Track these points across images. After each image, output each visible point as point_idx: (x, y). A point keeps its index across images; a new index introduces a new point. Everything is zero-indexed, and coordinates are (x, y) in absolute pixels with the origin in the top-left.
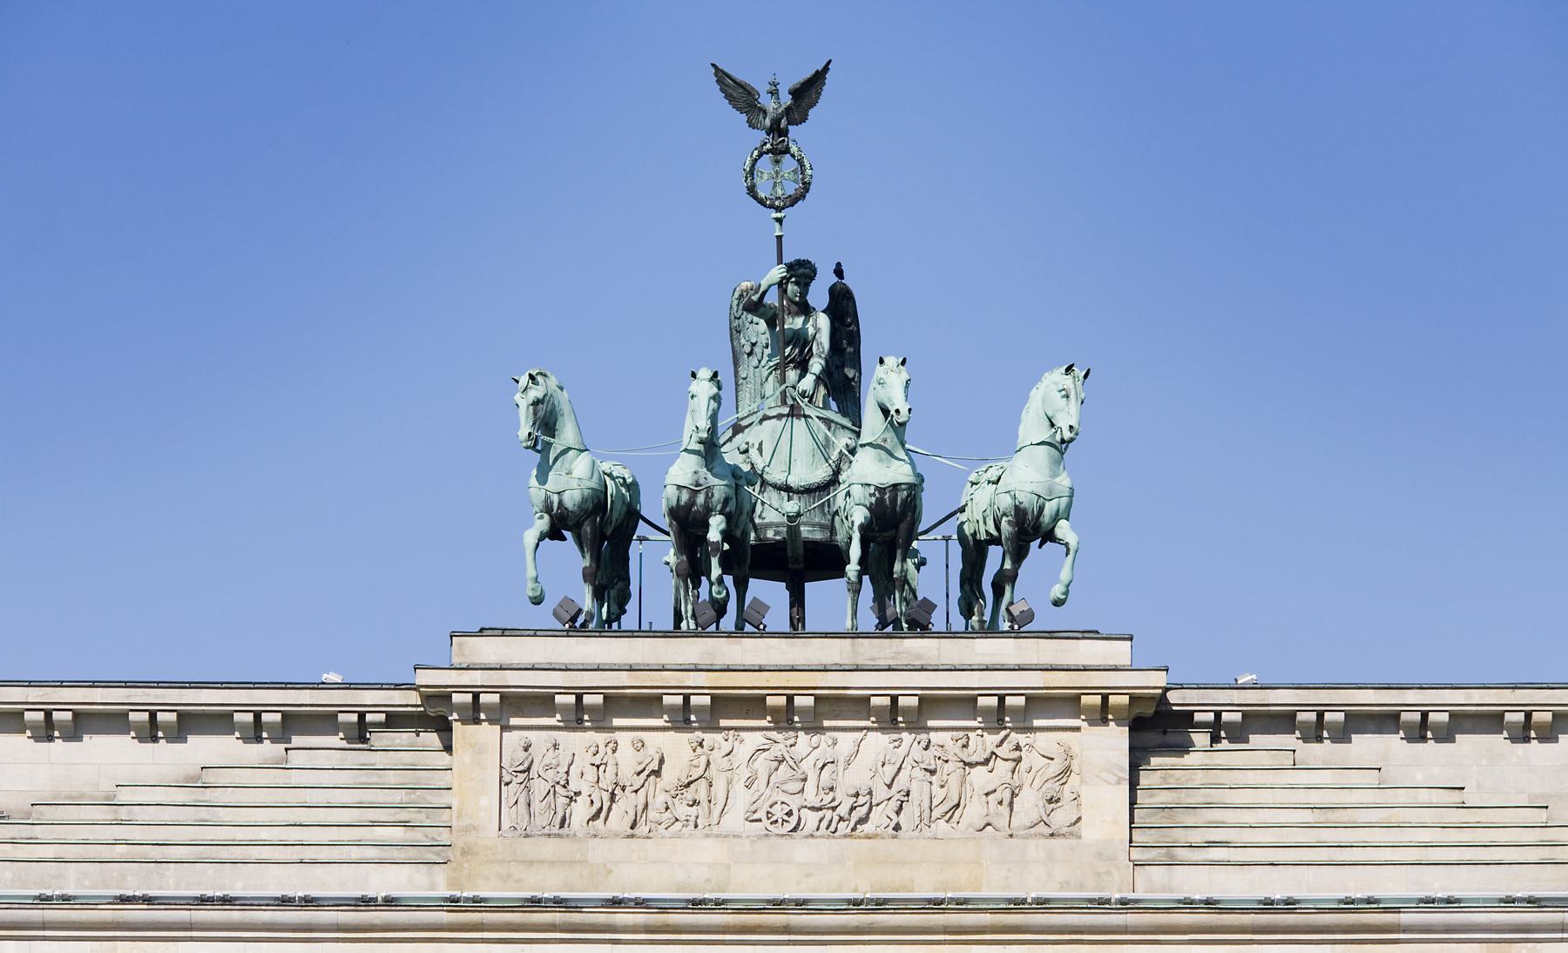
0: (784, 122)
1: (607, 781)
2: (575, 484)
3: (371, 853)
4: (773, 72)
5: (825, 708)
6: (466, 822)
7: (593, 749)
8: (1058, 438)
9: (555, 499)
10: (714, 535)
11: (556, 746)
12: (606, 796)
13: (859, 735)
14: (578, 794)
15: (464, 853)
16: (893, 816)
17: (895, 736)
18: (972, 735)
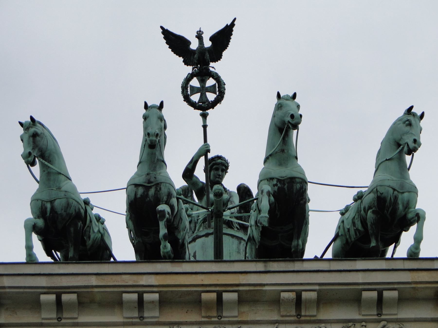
0: (207, 55)
2: (62, 195)
5: (245, 309)
8: (406, 149)
9: (49, 206)
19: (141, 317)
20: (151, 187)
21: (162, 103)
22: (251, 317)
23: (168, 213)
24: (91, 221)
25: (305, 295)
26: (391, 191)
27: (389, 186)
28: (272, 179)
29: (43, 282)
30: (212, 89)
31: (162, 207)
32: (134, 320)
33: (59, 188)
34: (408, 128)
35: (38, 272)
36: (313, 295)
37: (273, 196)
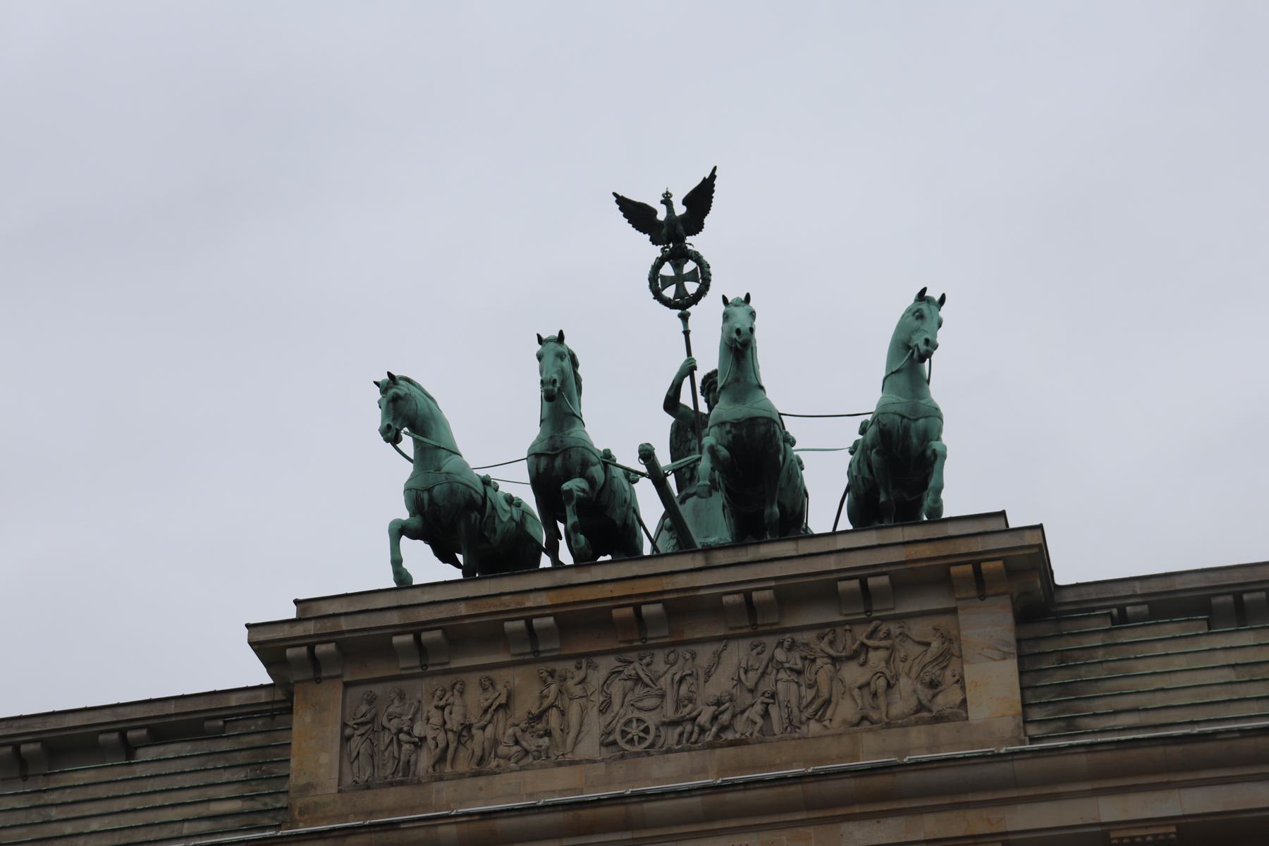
1: (455, 721)
2: (442, 478)
3: (204, 826)
4: (662, 186)
6: (302, 781)
7: (438, 693)
9: (426, 496)
10: (566, 486)
11: (402, 696)
12: (450, 735)
13: (717, 647)
14: (423, 739)
15: (301, 813)
16: (760, 721)
17: (756, 640)
18: (839, 630)
19: (536, 652)
20: (556, 455)
21: (561, 333)
22: (689, 635)
23: (583, 491)
24: (494, 508)
25: (755, 596)
26: (898, 419)
27: (895, 413)
28: (723, 423)
29: (394, 619)
30: (692, 276)
31: (575, 485)
32: (527, 657)
33: (439, 469)
34: (918, 323)
35: (394, 604)
36: (768, 594)
37: (727, 448)
